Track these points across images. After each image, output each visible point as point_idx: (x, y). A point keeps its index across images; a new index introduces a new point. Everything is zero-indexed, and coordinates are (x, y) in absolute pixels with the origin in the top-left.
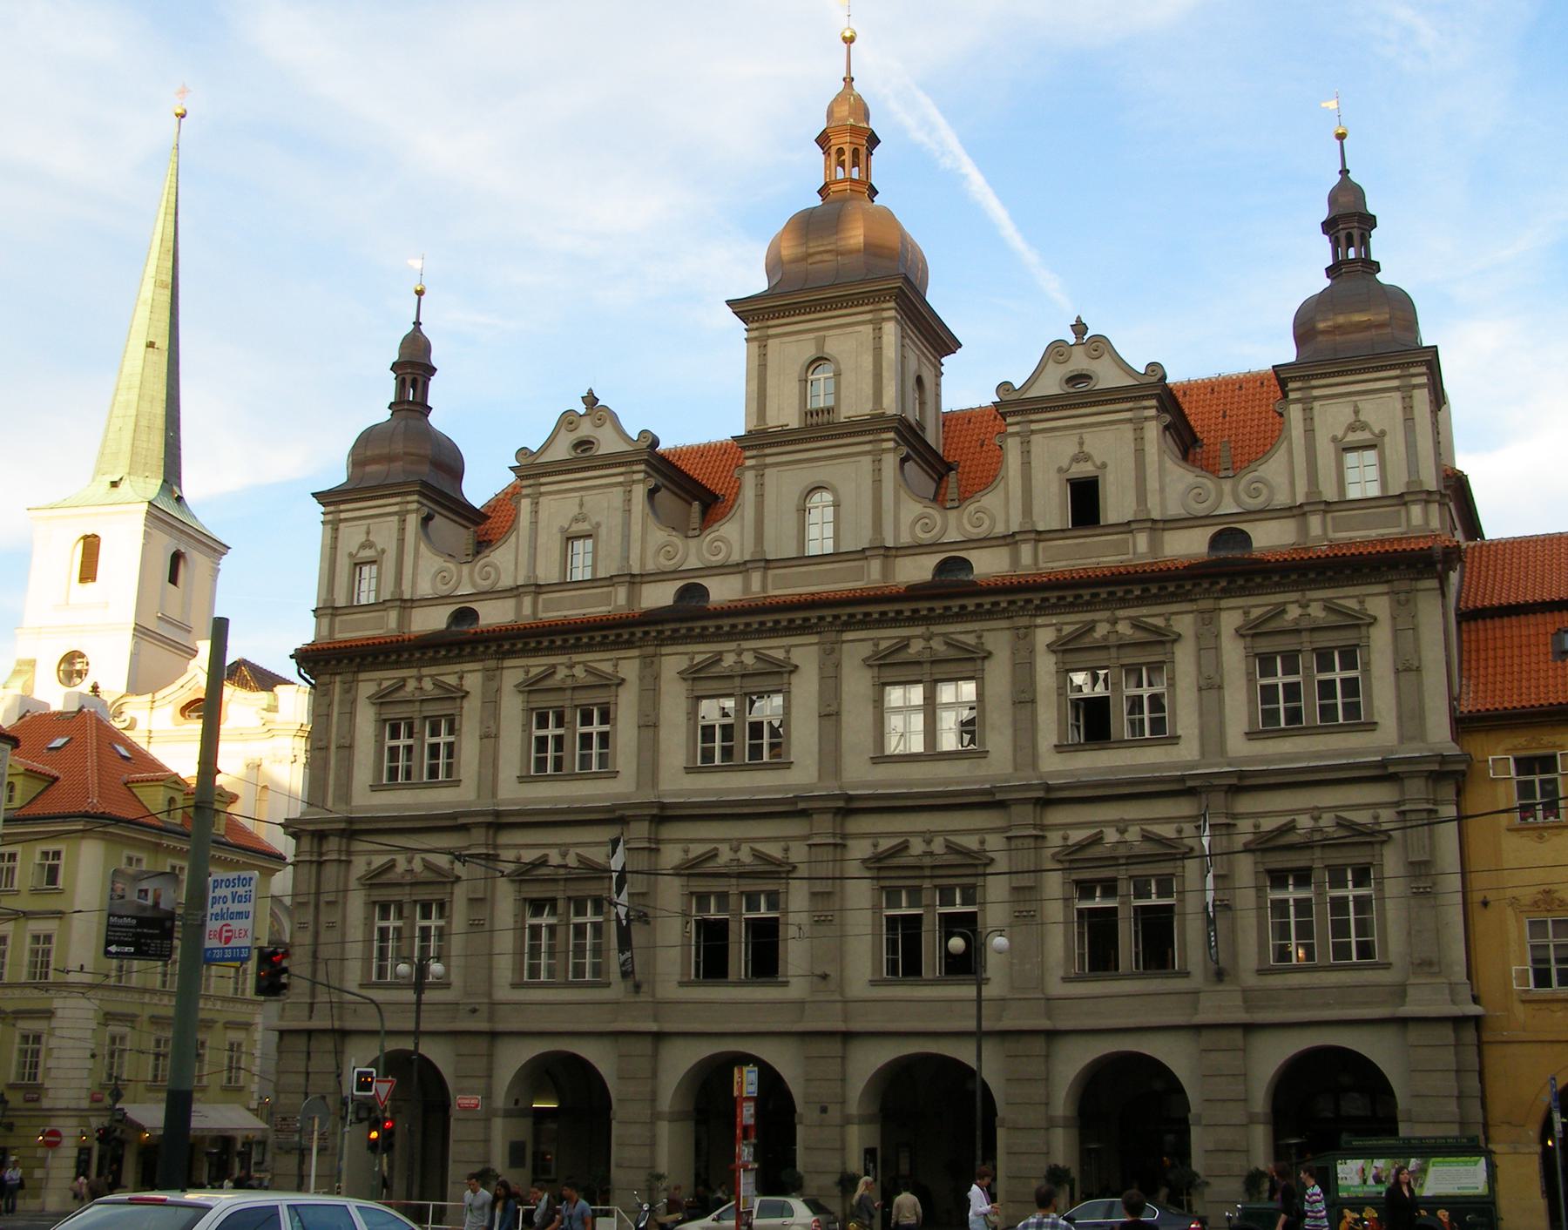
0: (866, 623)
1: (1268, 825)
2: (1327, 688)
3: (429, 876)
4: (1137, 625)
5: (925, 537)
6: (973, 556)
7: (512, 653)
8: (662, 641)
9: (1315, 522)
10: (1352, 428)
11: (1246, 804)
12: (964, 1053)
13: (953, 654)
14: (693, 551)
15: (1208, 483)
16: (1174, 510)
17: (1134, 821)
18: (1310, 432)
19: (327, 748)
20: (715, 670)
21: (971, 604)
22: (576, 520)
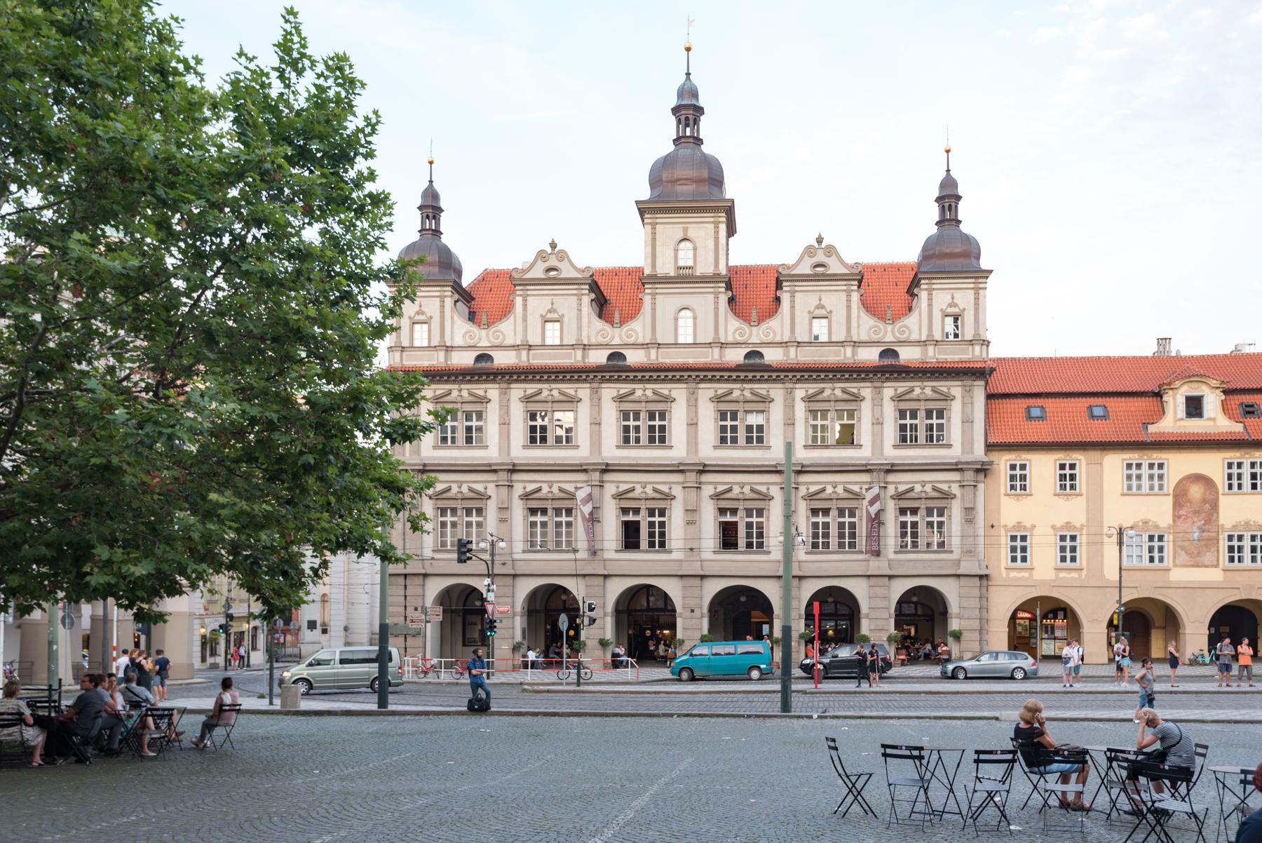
0: (712, 380)
1: (902, 488)
3: (472, 495)
4: (844, 391)
5: (739, 339)
7: (517, 381)
8: (603, 380)
9: (931, 349)
10: (950, 306)
11: (892, 478)
13: (754, 398)
15: (881, 325)
16: (864, 338)
17: (840, 483)
18: (930, 306)
20: (631, 398)
21: (766, 375)
22: (550, 311)
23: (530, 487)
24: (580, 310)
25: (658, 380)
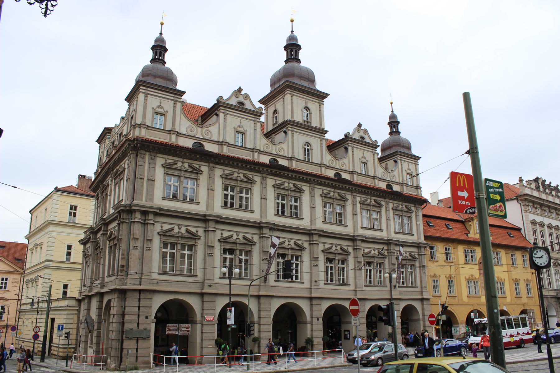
2: (241, 198)
4: (375, 201)
6: (342, 174)
12: (245, 301)
14: (274, 149)
19: (143, 179)
23: (226, 234)
25: (299, 180)
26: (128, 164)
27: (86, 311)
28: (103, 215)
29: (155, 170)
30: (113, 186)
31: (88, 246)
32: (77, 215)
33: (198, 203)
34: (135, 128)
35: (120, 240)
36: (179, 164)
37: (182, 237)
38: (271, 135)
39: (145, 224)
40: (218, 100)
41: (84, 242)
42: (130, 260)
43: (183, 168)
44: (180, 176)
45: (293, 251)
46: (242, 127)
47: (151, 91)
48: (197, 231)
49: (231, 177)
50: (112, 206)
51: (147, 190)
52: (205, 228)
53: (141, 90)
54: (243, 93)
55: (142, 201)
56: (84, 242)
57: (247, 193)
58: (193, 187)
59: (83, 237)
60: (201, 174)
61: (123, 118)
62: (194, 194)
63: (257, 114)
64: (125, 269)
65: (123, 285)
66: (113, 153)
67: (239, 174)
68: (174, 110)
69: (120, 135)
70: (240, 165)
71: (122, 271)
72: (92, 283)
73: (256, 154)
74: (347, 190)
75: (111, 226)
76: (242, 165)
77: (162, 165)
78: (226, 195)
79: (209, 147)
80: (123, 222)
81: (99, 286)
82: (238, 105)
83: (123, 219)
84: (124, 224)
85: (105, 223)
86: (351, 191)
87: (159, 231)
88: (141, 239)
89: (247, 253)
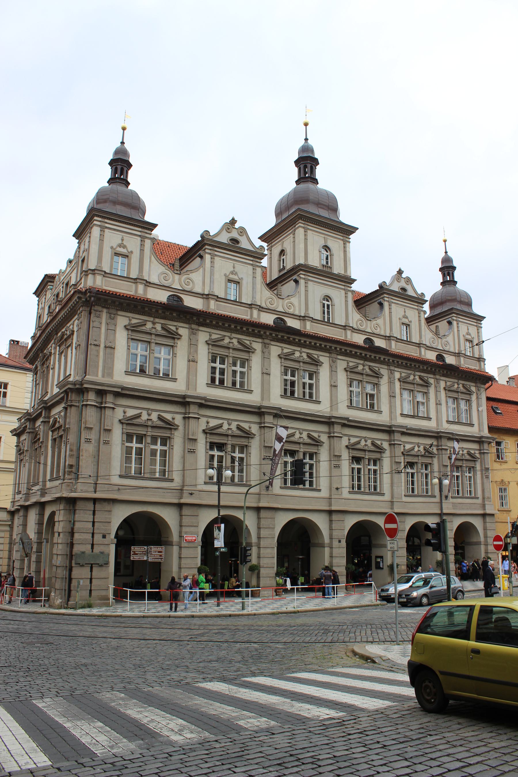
0: (345, 354)
4: (421, 378)
12: (239, 514)
14: (281, 304)
19: (99, 346)
23: (213, 423)
24: (254, 277)
25: (315, 348)
26: (78, 325)
27: (21, 527)
28: (43, 396)
29: (115, 333)
30: (57, 356)
31: (23, 438)
32: (8, 395)
33: (175, 380)
34: (87, 275)
35: (67, 430)
36: (149, 325)
37: (153, 427)
38: (276, 285)
39: (101, 408)
40: (202, 236)
41: (18, 433)
42: (81, 458)
43: (154, 330)
44: (149, 342)
45: (306, 447)
46: (236, 274)
47: (109, 224)
48: (173, 419)
49: (221, 343)
50: (56, 383)
51: (105, 361)
52: (185, 413)
53: (95, 222)
54: (237, 226)
55: (97, 376)
56: (18, 433)
57: (242, 366)
58: (168, 357)
59: (16, 425)
60: (178, 339)
61: (70, 261)
62: (169, 366)
63: (256, 255)
64: (74, 470)
65: (72, 491)
66: (57, 310)
67: (231, 339)
68: (142, 250)
69: (67, 284)
70: (233, 327)
71: (70, 473)
72: (29, 489)
73: (255, 312)
74: (383, 362)
75: (55, 411)
76: (236, 327)
77: (125, 326)
78: (214, 369)
79: (190, 302)
80: (71, 406)
81: (39, 493)
82: (228, 243)
83: (71, 401)
84: (73, 408)
85: (46, 407)
86: (388, 364)
87: (121, 417)
88: (96, 429)
89: (243, 448)
